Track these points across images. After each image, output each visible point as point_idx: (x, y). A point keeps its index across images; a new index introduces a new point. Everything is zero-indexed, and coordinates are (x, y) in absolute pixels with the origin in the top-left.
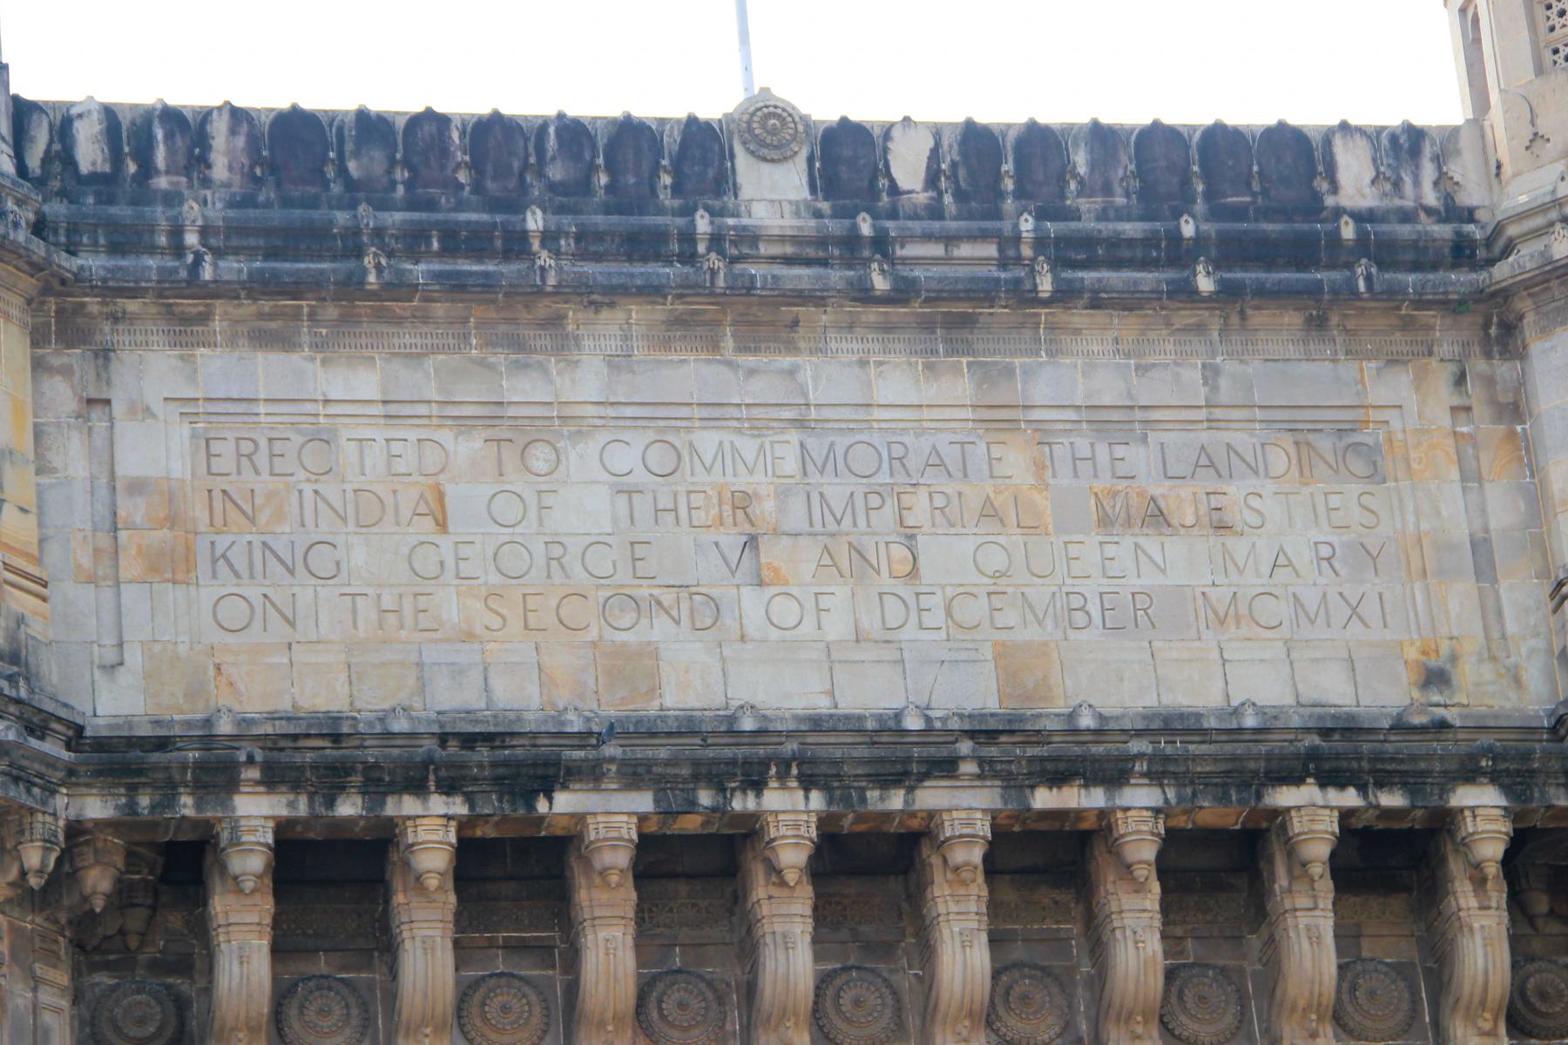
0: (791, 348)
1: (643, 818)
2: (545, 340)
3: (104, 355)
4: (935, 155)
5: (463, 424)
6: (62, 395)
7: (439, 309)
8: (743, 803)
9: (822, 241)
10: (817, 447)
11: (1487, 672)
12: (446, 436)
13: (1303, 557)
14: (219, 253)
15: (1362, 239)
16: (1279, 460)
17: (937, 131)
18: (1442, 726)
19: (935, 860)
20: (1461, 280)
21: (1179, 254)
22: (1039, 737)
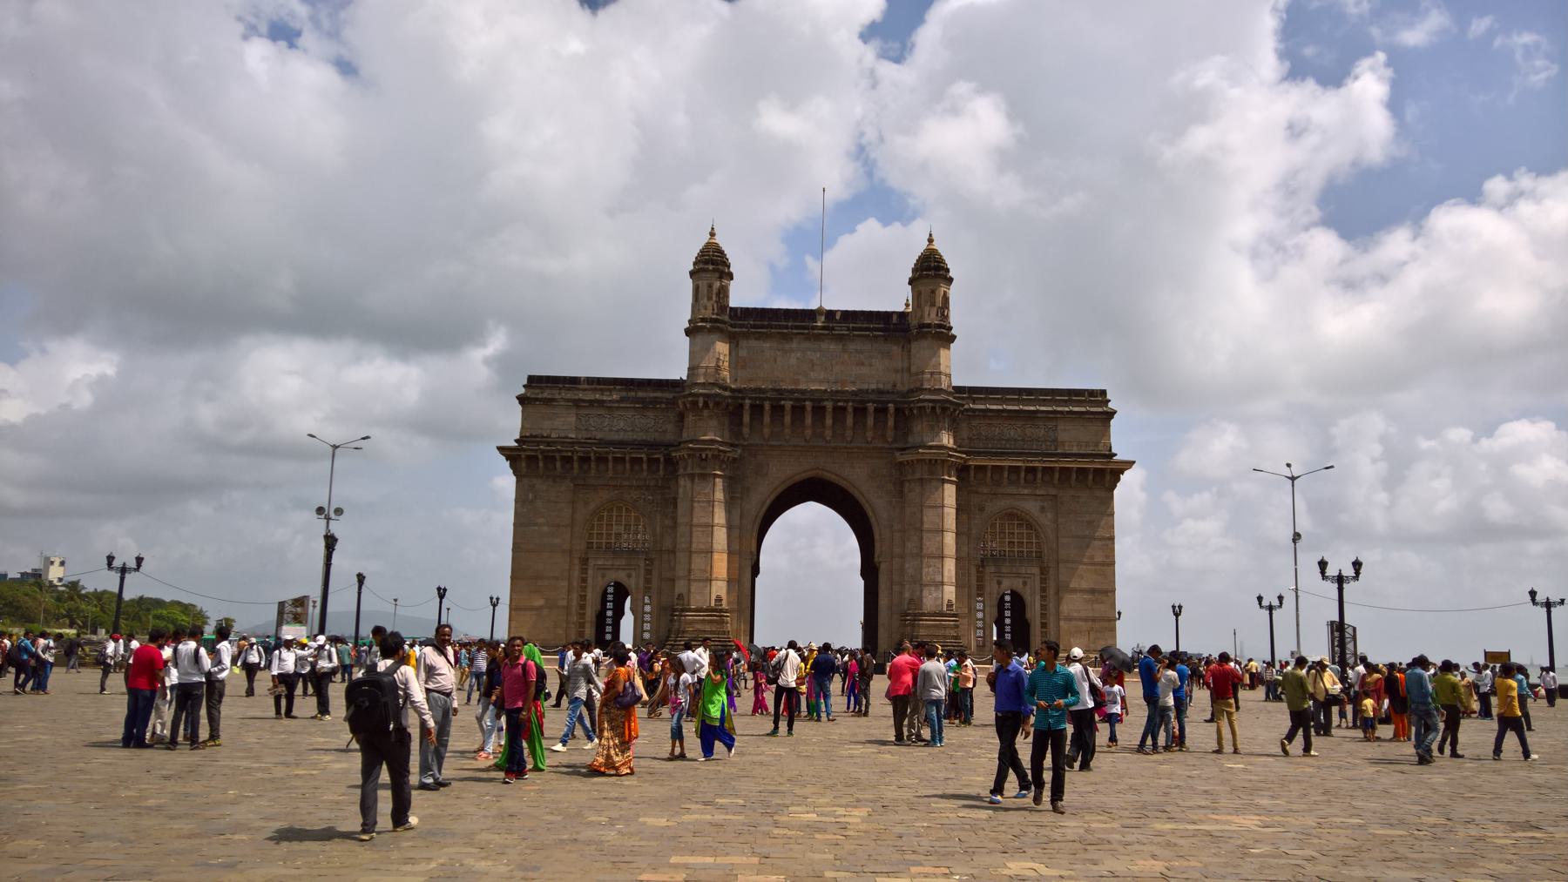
3: (738, 341)
5: (779, 350)
17: (842, 311)
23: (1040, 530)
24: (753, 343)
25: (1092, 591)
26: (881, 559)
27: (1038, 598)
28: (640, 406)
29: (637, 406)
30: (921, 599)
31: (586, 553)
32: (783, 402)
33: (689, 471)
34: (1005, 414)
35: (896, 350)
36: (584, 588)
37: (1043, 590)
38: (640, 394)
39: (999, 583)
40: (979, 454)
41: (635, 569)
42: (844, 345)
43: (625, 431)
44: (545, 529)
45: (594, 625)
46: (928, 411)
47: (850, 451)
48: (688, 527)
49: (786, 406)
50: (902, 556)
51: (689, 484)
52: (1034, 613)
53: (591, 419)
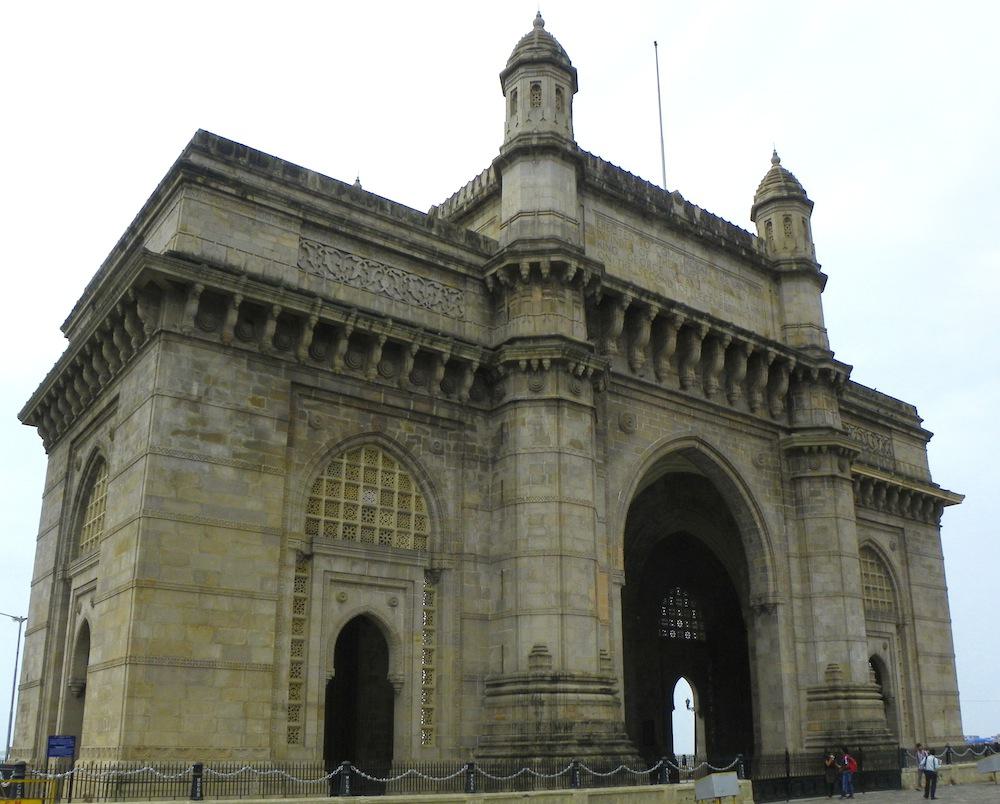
1: (686, 319)
4: (701, 213)
5: (637, 234)
8: (700, 321)
16: (747, 290)
19: (718, 342)
23: (892, 574)
24: (602, 208)
25: (941, 656)
26: (779, 600)
27: (898, 665)
28: (423, 257)
29: (417, 255)
30: (848, 663)
32: (675, 311)
33: (550, 392)
34: (854, 412)
35: (764, 284)
38: (417, 238)
41: (404, 589)
43: (389, 297)
44: (228, 473)
45: (323, 711)
46: (833, 377)
47: (733, 418)
48: (554, 507)
49: (678, 318)
50: (807, 598)
51: (548, 420)
53: (328, 259)
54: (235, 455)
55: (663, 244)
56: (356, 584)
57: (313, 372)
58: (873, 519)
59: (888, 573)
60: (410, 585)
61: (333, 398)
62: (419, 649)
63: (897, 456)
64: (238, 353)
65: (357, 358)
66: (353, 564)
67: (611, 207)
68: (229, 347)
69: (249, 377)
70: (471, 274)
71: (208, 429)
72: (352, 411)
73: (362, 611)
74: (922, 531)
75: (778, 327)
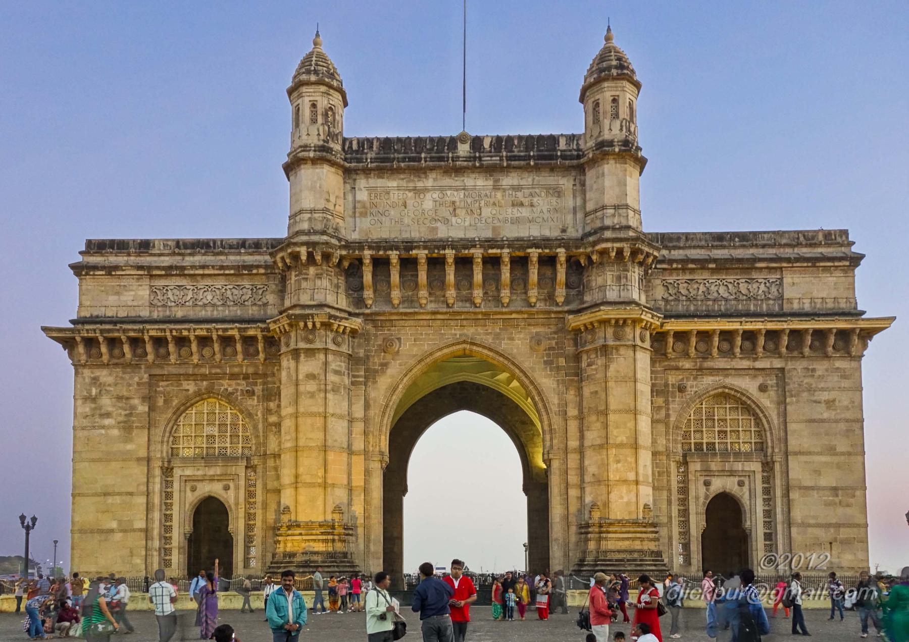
0: (464, 176)
2: (423, 176)
3: (355, 180)
5: (410, 191)
6: (348, 187)
7: (407, 171)
9: (470, 157)
10: (467, 194)
11: (573, 230)
12: (407, 192)
13: (545, 210)
14: (371, 162)
15: (561, 155)
16: (543, 194)
18: (563, 239)
20: (575, 162)
21: (529, 158)
22: (497, 241)
23: (761, 415)
31: (169, 462)
35: (566, 183)
36: (169, 506)
37: (767, 491)
39: (707, 484)
40: (678, 316)
42: (496, 181)
44: (115, 432)
52: (755, 523)
54: (119, 423)
55: (442, 189)
56: (202, 480)
57: (160, 366)
58: (729, 367)
59: (757, 414)
60: (236, 477)
61: (177, 378)
62: (242, 514)
63: (787, 294)
64: (116, 365)
65: (184, 351)
66: (198, 470)
67: (383, 178)
68: (108, 365)
69: (122, 378)
70: (269, 272)
71: (103, 411)
72: (190, 382)
73: (207, 495)
74: (821, 367)
75: (580, 215)
